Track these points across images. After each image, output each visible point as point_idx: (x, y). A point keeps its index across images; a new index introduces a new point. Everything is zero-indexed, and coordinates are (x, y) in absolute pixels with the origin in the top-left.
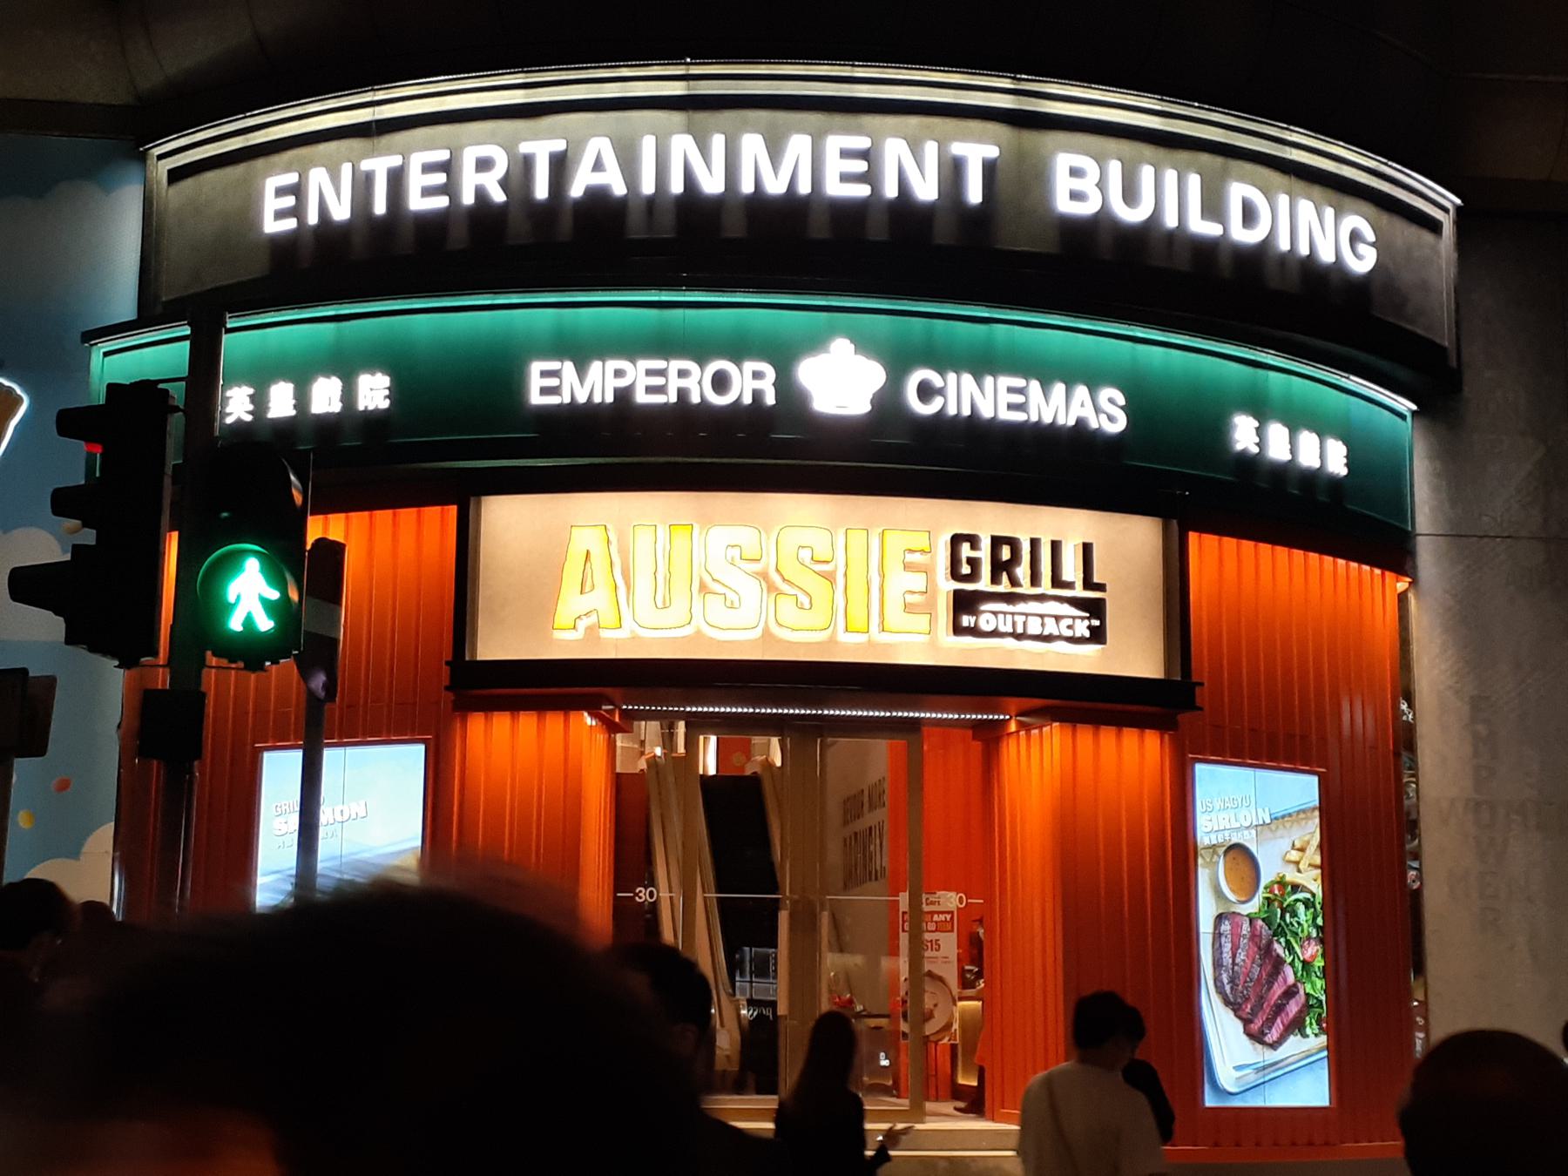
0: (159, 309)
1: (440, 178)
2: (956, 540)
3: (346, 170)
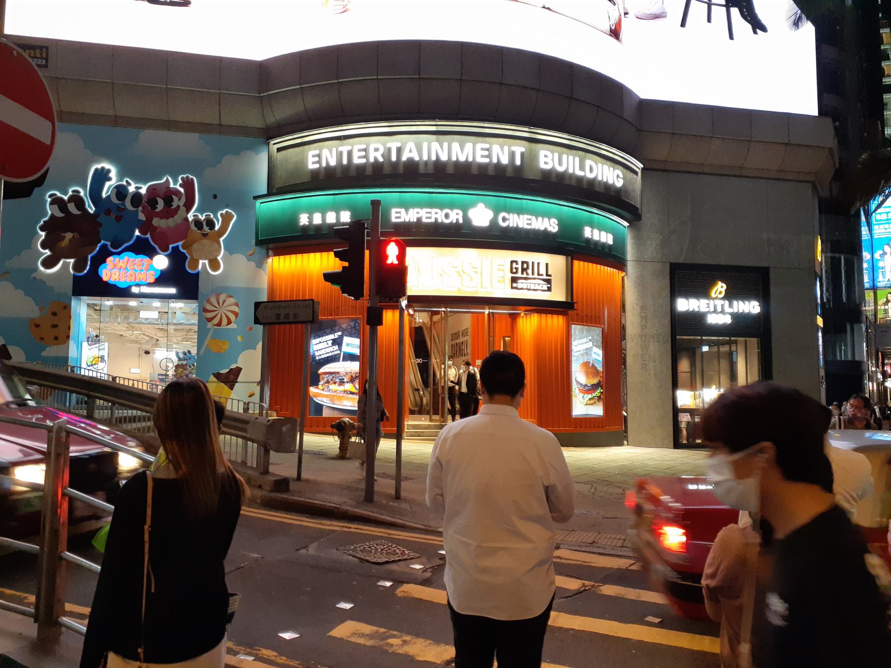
0: (274, 191)
1: (363, 153)
2: (512, 262)
3: (334, 150)
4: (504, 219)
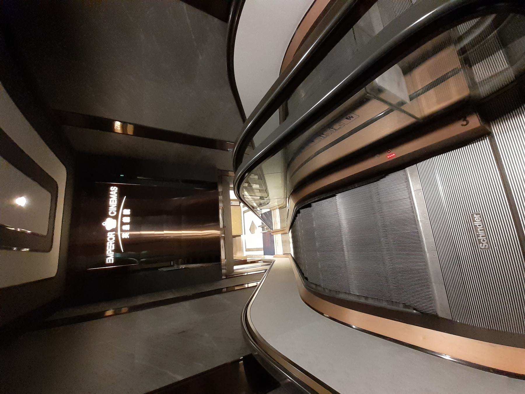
4: (112, 213)
